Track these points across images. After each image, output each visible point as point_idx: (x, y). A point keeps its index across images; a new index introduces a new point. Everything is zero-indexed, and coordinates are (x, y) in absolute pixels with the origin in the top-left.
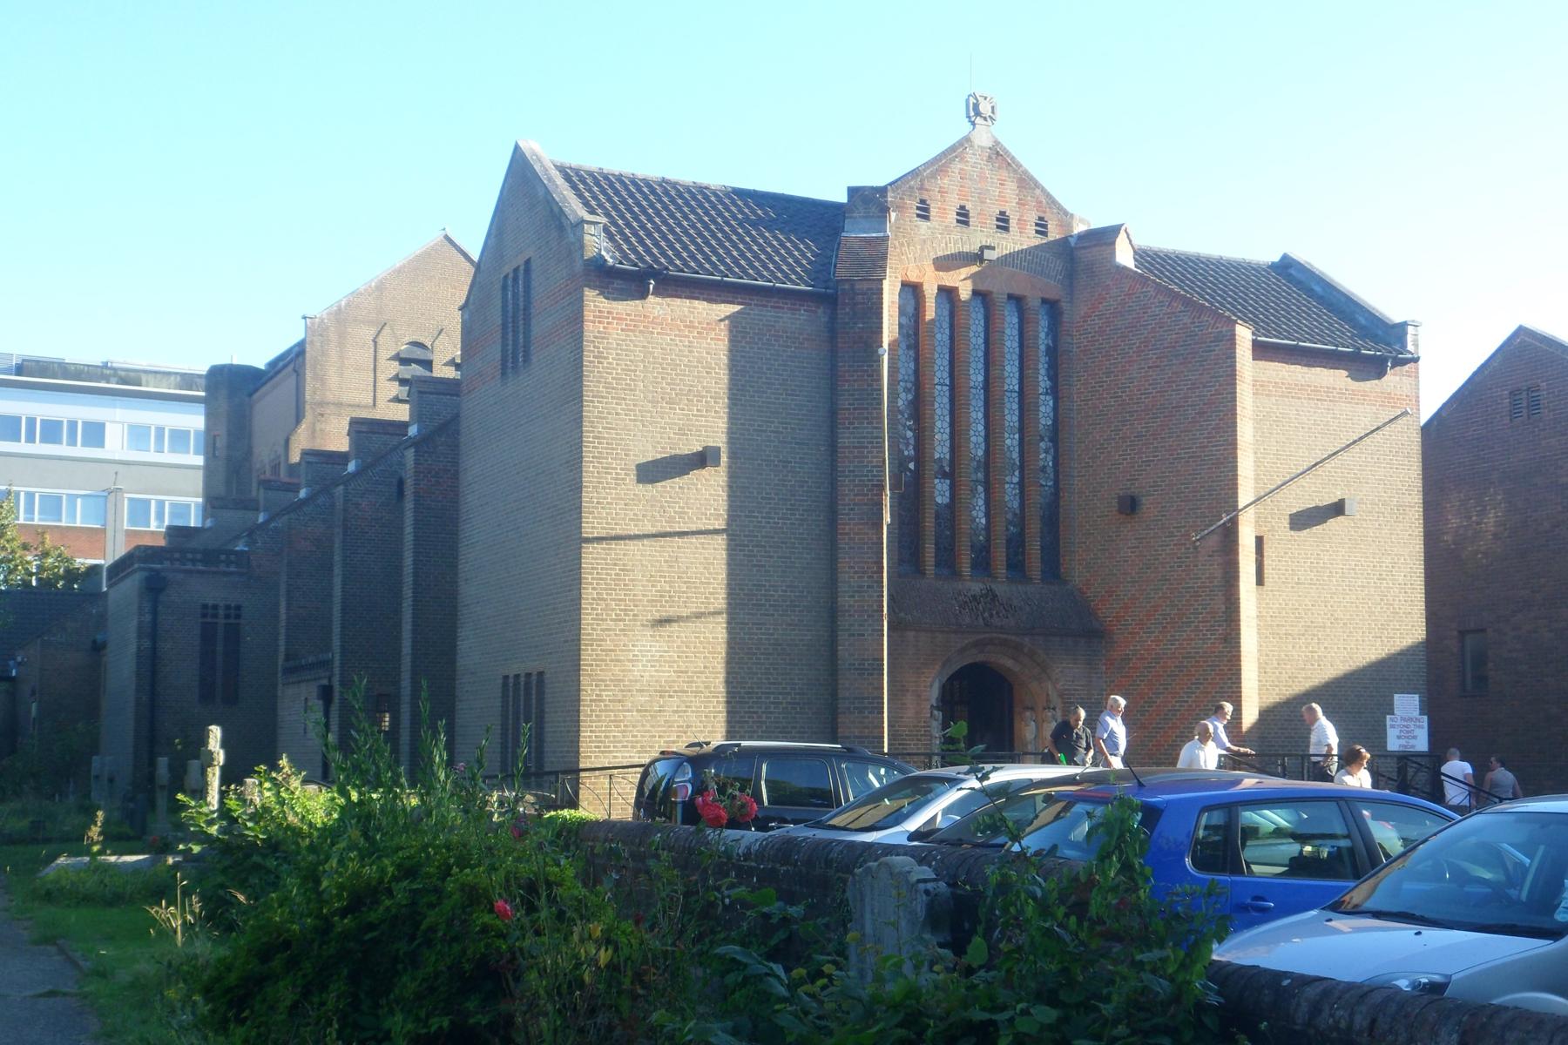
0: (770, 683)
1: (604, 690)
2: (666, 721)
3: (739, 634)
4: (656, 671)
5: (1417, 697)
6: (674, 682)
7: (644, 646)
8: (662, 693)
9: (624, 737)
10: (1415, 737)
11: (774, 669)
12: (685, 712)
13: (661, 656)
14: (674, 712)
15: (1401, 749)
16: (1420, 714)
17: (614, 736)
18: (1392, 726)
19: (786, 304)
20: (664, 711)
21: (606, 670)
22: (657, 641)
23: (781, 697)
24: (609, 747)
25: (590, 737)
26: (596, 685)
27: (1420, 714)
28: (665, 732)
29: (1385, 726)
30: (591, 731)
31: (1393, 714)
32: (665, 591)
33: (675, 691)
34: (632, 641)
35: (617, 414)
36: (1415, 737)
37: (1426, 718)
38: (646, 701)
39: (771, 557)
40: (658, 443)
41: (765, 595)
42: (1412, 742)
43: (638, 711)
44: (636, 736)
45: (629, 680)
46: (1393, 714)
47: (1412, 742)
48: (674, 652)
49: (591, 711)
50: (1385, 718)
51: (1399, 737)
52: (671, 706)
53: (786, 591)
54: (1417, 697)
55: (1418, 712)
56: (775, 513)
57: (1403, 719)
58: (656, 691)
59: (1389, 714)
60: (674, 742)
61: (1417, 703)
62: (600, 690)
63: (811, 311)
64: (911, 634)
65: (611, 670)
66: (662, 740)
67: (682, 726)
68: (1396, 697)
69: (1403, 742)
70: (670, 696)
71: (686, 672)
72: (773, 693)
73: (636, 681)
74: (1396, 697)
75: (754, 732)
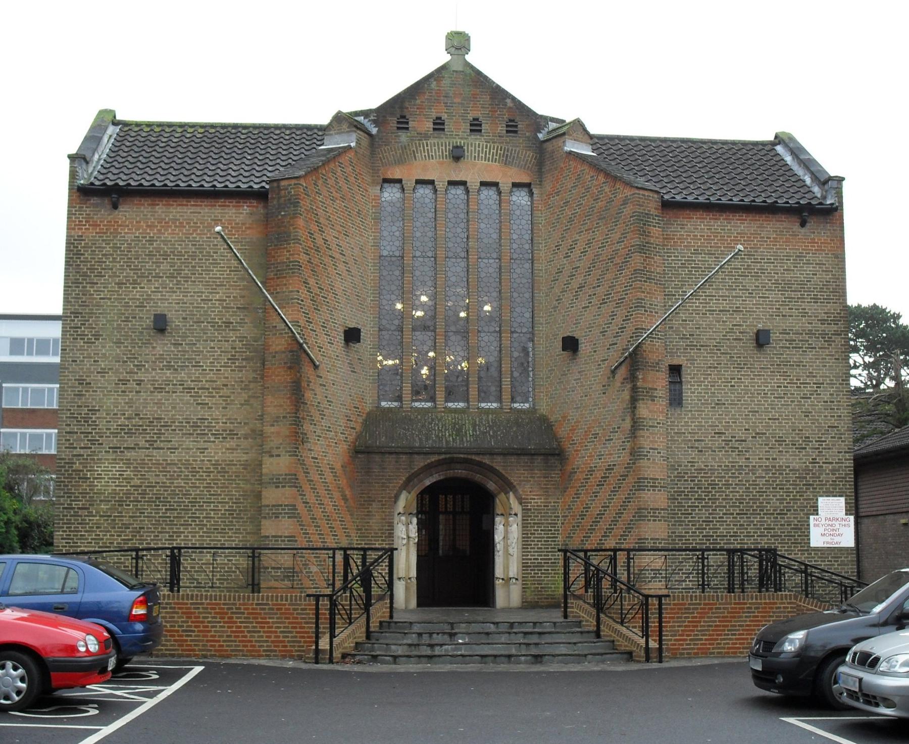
0: (210, 495)
3: (185, 457)
5: (842, 499)
8: (120, 502)
11: (214, 484)
12: (140, 517)
13: (120, 475)
15: (826, 545)
16: (846, 514)
17: (81, 535)
19: (232, 202)
22: (117, 463)
23: (220, 505)
24: (77, 543)
25: (63, 535)
26: (68, 497)
27: (846, 514)
29: (809, 525)
30: (63, 531)
31: (817, 514)
32: (125, 426)
34: (97, 463)
37: (852, 518)
39: (213, 397)
41: (208, 427)
42: (837, 539)
44: (99, 535)
46: (817, 514)
47: (837, 539)
49: (63, 516)
50: (809, 518)
53: (226, 423)
54: (842, 499)
56: (218, 363)
59: (813, 514)
60: (129, 540)
62: (71, 501)
63: (254, 206)
66: (119, 538)
67: (136, 528)
68: (820, 499)
69: (828, 539)
70: (126, 505)
71: (141, 486)
72: (214, 502)
74: (820, 499)
75: (196, 532)
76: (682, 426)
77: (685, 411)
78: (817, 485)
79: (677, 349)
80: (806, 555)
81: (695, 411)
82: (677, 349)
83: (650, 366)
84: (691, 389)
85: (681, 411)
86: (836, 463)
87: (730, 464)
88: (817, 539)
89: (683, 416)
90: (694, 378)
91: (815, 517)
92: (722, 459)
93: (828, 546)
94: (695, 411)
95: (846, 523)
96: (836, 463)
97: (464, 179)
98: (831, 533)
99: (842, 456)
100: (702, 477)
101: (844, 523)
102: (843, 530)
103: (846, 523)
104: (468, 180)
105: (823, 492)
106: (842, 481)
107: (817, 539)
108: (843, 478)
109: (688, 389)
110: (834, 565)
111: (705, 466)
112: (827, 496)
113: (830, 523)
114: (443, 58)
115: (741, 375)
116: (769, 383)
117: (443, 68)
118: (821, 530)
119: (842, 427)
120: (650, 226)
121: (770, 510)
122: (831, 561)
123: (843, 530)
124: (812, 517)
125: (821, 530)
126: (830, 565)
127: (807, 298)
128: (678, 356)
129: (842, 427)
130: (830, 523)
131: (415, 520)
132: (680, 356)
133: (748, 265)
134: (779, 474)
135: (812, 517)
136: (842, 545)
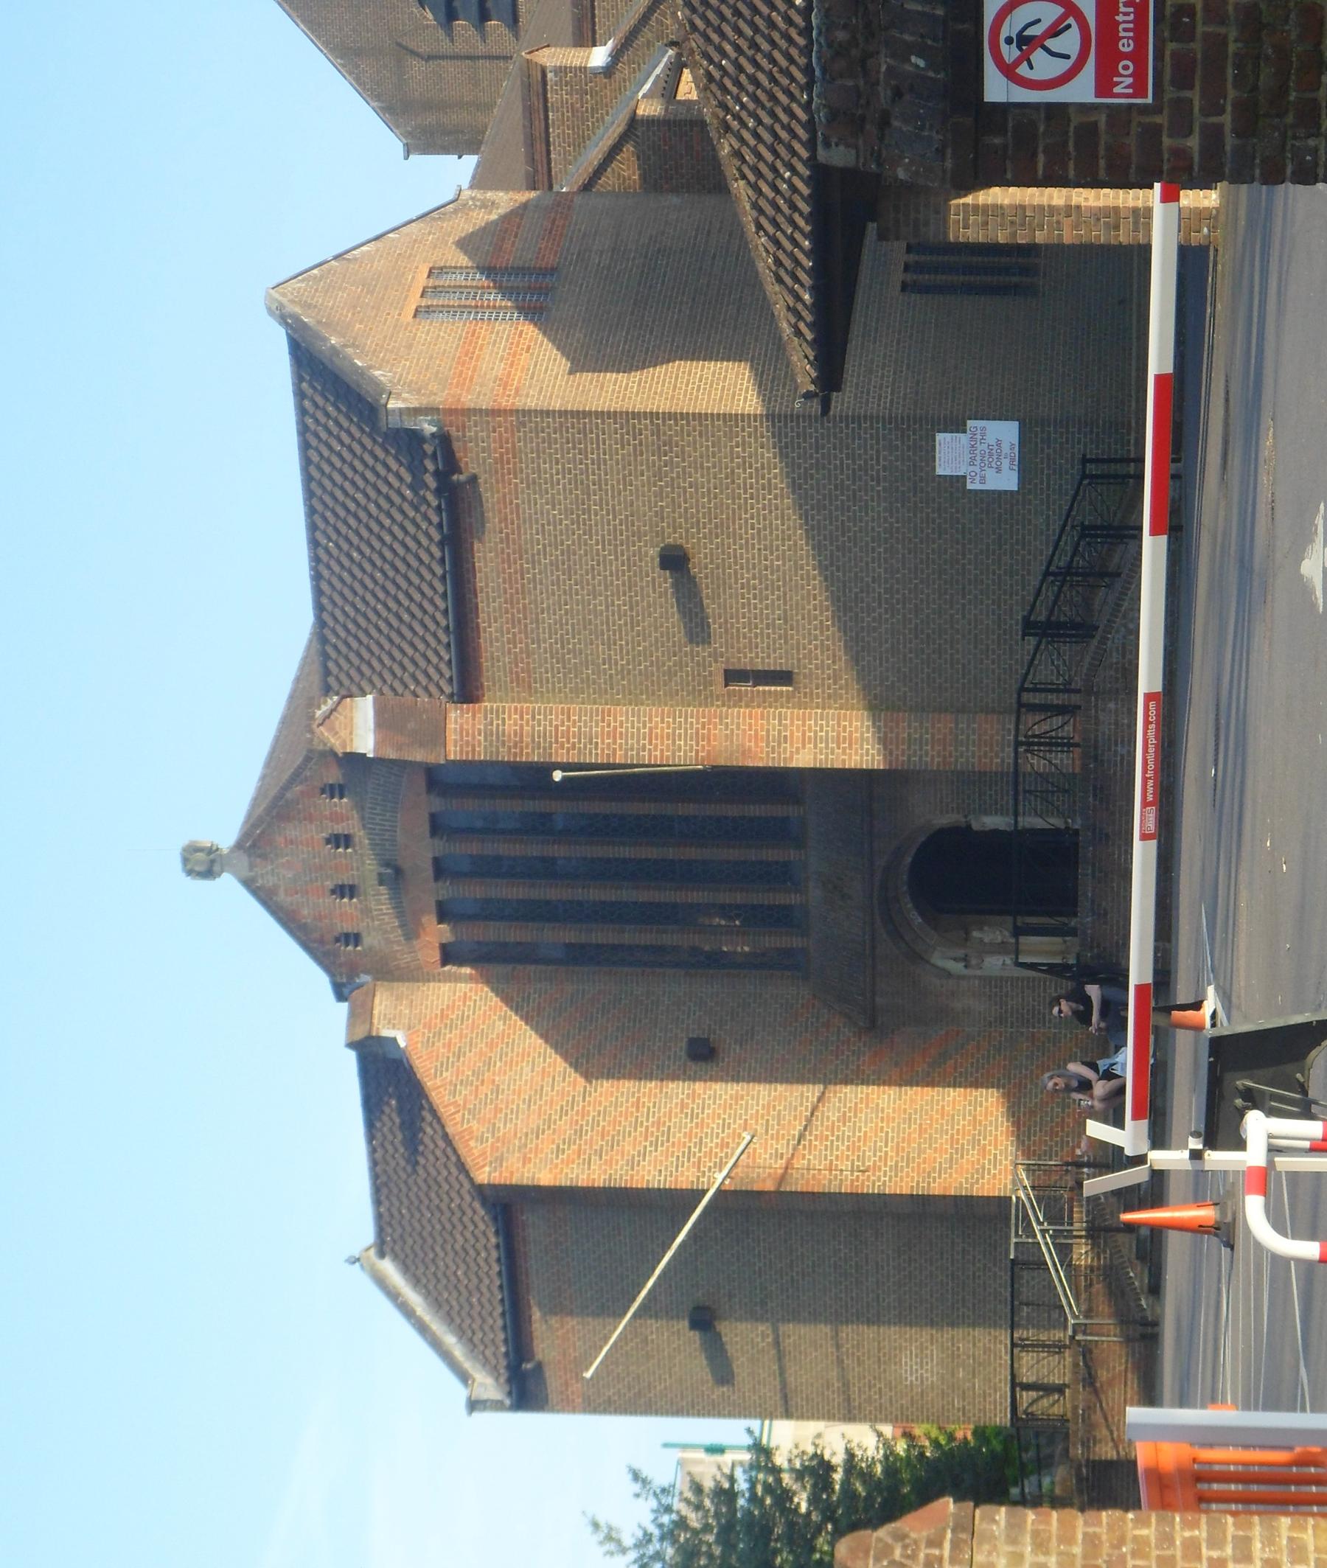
1: (953, 1405)
2: (985, 1353)
4: (932, 1360)
5: (940, 437)
6: (942, 1346)
7: (906, 1371)
9: (1000, 1390)
10: (999, 443)
13: (916, 1357)
14: (974, 1345)
18: (983, 480)
20: (974, 1355)
21: (932, 1404)
22: (901, 1360)
27: (965, 432)
28: (995, 1354)
31: (964, 477)
33: (953, 1345)
35: (666, 1388)
36: (999, 443)
37: (970, 423)
38: (964, 1370)
40: (690, 1354)
42: (1006, 448)
43: (974, 1377)
45: (943, 1383)
46: (964, 477)
47: (1006, 448)
48: (911, 1345)
51: (999, 470)
52: (969, 1348)
54: (940, 437)
55: (961, 435)
57: (972, 463)
58: (953, 1362)
61: (948, 436)
64: (878, 1000)
65: (932, 1400)
68: (939, 471)
69: (1005, 463)
73: (943, 1378)
74: (939, 471)
76: (823, 673)
77: (799, 668)
78: (915, 475)
79: (699, 675)
80: (1031, 497)
81: (798, 654)
82: (699, 675)
83: (732, 741)
84: (762, 658)
85: (798, 674)
86: (878, 443)
87: (884, 606)
88: (1006, 480)
89: (807, 671)
90: (745, 654)
91: (968, 481)
92: (874, 618)
93: (1016, 463)
94: (798, 654)
95: (979, 431)
96: (878, 443)
97: (430, 862)
98: (995, 457)
99: (866, 433)
100: (905, 647)
101: (979, 437)
102: (990, 439)
103: (979, 431)
104: (430, 855)
105: (927, 465)
106: (909, 436)
107: (1006, 480)
108: (902, 436)
109: (763, 663)
110: (1048, 455)
111: (886, 642)
112: (935, 461)
113: (978, 458)
114: (228, 886)
115: (736, 583)
116: (747, 542)
117: (249, 884)
118: (990, 473)
119: (816, 432)
120: (504, 730)
121: (957, 550)
122: (1042, 458)
123: (990, 439)
124: (970, 486)
125: (990, 473)
126: (1049, 459)
127: (600, 475)
128: (711, 674)
129: (816, 432)
130: (978, 458)
131: (976, 934)
132: (710, 672)
133: (552, 565)
134: (897, 532)
135: (970, 486)
136: (1016, 442)
